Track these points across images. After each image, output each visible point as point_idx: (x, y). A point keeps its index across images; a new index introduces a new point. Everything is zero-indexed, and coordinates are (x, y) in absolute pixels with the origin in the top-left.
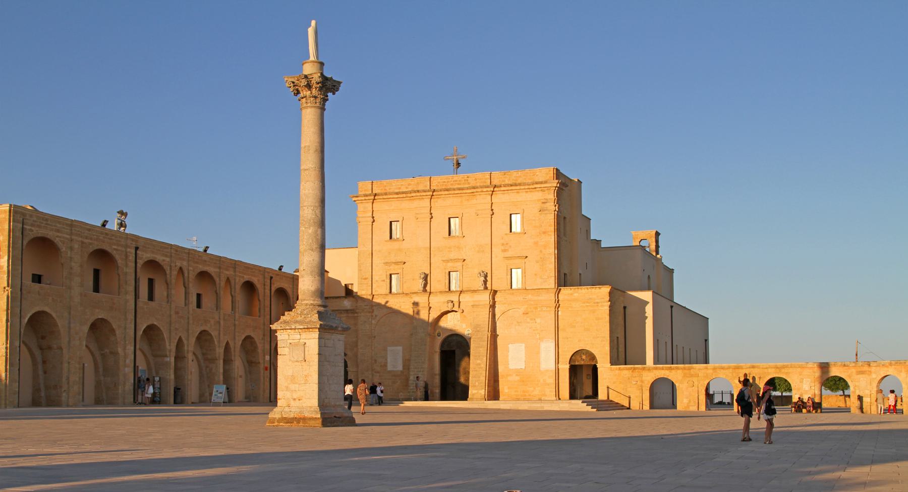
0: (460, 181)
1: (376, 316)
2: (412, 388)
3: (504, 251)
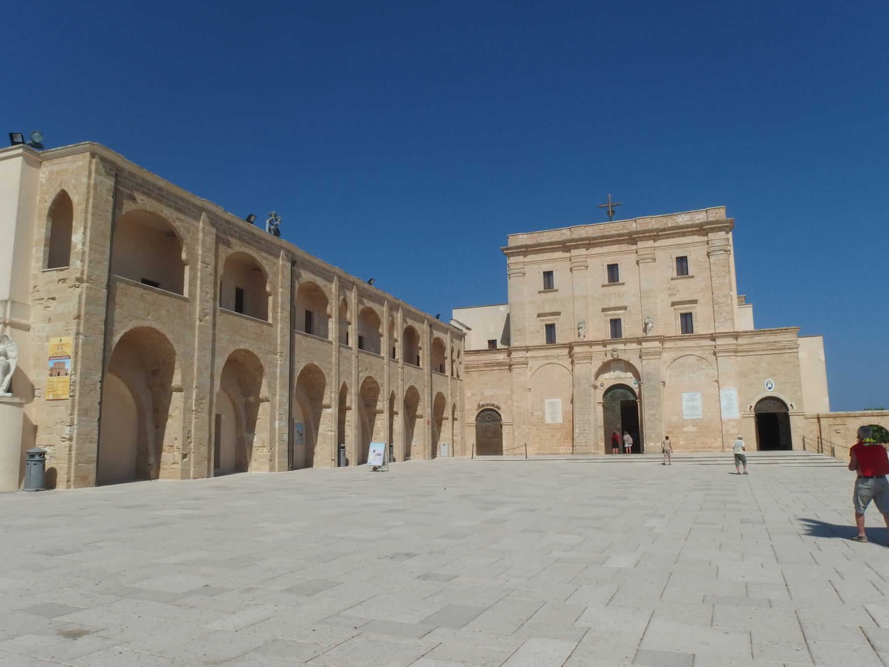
0: (617, 227)
1: (531, 367)
2: (578, 441)
3: (670, 295)
